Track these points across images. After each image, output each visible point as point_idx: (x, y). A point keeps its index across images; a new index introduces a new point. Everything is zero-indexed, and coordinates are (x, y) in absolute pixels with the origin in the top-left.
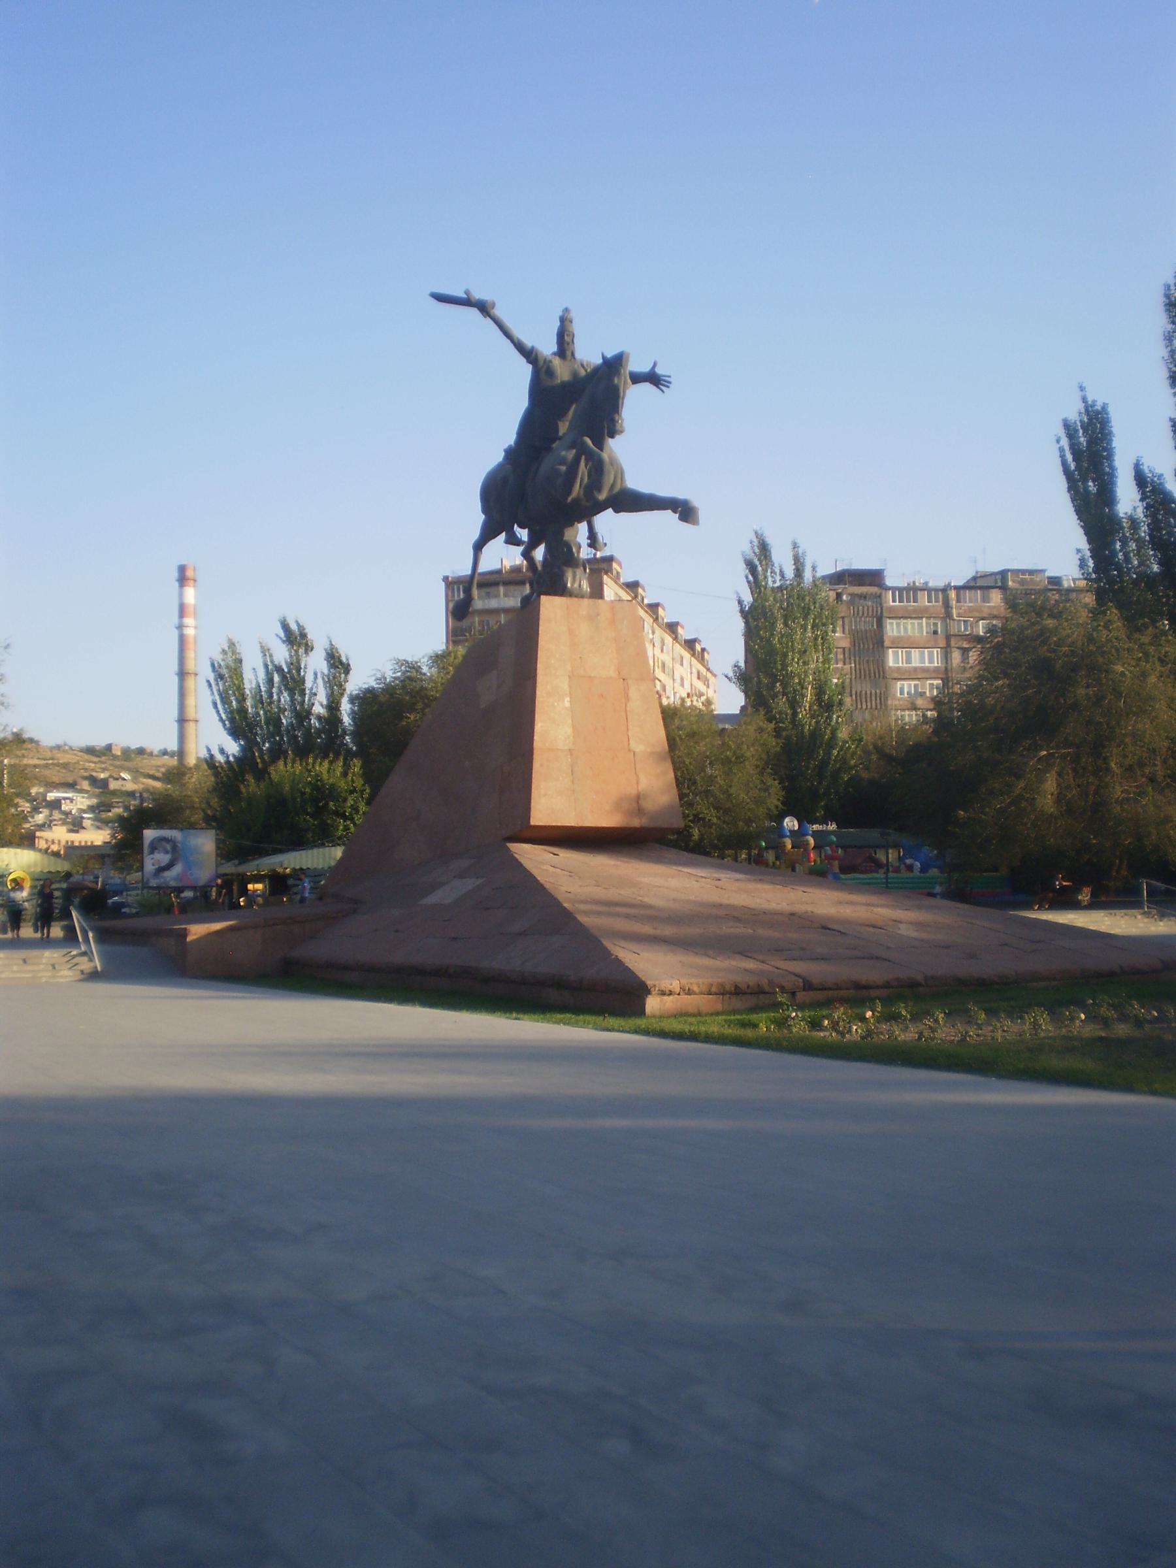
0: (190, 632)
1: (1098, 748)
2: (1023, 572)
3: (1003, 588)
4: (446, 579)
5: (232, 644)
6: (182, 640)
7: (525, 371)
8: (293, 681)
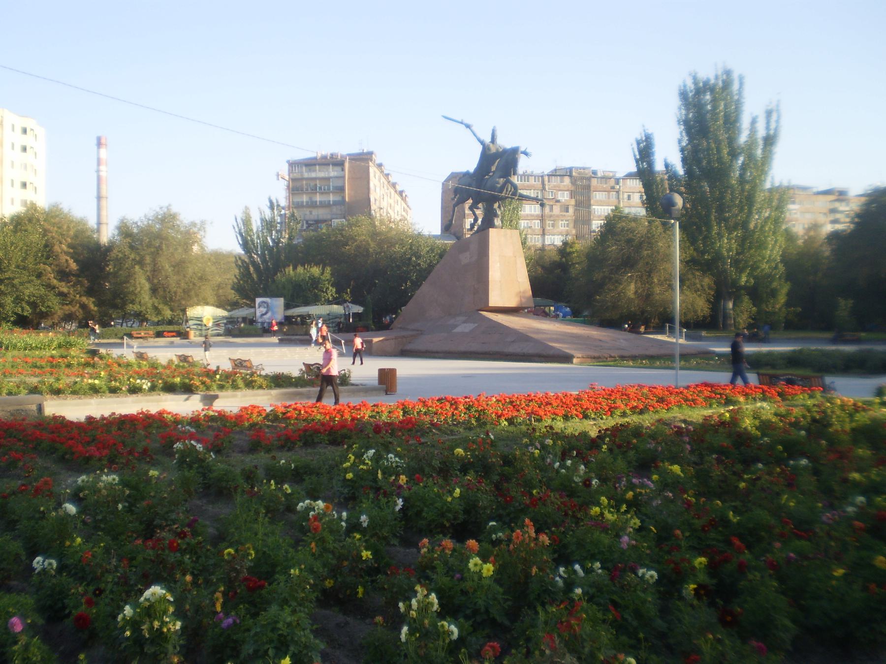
0: (103, 174)
1: (649, 273)
2: (580, 168)
3: (571, 176)
4: (288, 162)
6: (99, 179)
7: (480, 148)
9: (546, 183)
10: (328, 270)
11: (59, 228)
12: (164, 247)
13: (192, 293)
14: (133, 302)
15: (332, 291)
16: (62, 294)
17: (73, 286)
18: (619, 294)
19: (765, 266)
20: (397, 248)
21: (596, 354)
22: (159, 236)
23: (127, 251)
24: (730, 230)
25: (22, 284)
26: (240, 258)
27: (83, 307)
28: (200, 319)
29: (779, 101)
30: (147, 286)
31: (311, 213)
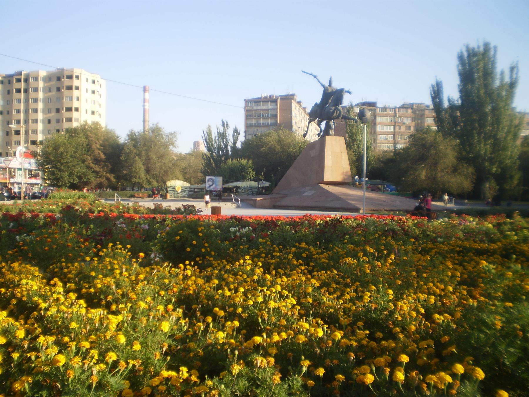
2: (418, 104)
3: (412, 108)
4: (245, 100)
5: (209, 126)
7: (322, 89)
8: (222, 136)
9: (397, 112)
10: (251, 161)
11: (96, 135)
12: (153, 146)
13: (169, 173)
14: (135, 177)
15: (253, 174)
16: (95, 172)
17: (103, 167)
18: (416, 176)
19: (508, 161)
20: (291, 149)
21: (375, 208)
22: (150, 140)
23: (132, 148)
24: (486, 139)
25: (74, 166)
26: (205, 154)
27: (108, 179)
28: (174, 188)
29: (518, 61)
30: (143, 168)
31: (257, 130)
